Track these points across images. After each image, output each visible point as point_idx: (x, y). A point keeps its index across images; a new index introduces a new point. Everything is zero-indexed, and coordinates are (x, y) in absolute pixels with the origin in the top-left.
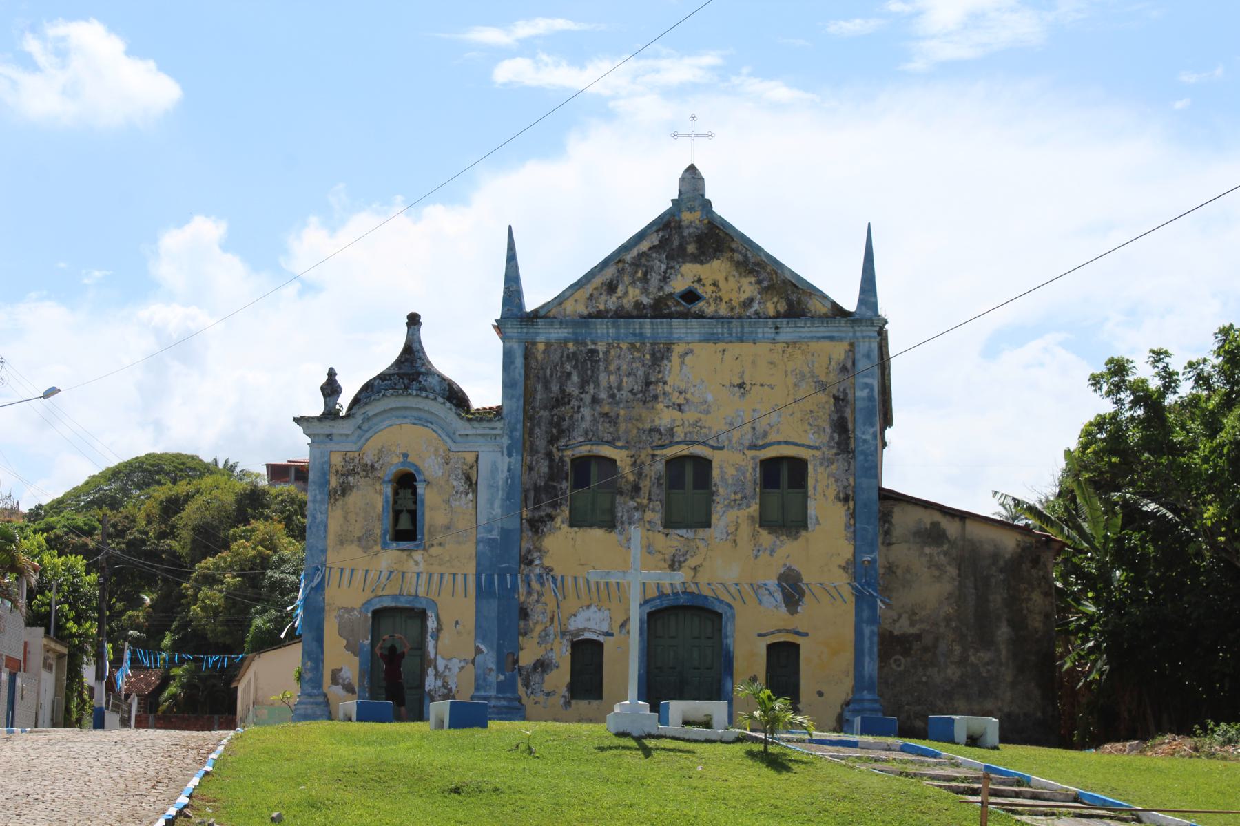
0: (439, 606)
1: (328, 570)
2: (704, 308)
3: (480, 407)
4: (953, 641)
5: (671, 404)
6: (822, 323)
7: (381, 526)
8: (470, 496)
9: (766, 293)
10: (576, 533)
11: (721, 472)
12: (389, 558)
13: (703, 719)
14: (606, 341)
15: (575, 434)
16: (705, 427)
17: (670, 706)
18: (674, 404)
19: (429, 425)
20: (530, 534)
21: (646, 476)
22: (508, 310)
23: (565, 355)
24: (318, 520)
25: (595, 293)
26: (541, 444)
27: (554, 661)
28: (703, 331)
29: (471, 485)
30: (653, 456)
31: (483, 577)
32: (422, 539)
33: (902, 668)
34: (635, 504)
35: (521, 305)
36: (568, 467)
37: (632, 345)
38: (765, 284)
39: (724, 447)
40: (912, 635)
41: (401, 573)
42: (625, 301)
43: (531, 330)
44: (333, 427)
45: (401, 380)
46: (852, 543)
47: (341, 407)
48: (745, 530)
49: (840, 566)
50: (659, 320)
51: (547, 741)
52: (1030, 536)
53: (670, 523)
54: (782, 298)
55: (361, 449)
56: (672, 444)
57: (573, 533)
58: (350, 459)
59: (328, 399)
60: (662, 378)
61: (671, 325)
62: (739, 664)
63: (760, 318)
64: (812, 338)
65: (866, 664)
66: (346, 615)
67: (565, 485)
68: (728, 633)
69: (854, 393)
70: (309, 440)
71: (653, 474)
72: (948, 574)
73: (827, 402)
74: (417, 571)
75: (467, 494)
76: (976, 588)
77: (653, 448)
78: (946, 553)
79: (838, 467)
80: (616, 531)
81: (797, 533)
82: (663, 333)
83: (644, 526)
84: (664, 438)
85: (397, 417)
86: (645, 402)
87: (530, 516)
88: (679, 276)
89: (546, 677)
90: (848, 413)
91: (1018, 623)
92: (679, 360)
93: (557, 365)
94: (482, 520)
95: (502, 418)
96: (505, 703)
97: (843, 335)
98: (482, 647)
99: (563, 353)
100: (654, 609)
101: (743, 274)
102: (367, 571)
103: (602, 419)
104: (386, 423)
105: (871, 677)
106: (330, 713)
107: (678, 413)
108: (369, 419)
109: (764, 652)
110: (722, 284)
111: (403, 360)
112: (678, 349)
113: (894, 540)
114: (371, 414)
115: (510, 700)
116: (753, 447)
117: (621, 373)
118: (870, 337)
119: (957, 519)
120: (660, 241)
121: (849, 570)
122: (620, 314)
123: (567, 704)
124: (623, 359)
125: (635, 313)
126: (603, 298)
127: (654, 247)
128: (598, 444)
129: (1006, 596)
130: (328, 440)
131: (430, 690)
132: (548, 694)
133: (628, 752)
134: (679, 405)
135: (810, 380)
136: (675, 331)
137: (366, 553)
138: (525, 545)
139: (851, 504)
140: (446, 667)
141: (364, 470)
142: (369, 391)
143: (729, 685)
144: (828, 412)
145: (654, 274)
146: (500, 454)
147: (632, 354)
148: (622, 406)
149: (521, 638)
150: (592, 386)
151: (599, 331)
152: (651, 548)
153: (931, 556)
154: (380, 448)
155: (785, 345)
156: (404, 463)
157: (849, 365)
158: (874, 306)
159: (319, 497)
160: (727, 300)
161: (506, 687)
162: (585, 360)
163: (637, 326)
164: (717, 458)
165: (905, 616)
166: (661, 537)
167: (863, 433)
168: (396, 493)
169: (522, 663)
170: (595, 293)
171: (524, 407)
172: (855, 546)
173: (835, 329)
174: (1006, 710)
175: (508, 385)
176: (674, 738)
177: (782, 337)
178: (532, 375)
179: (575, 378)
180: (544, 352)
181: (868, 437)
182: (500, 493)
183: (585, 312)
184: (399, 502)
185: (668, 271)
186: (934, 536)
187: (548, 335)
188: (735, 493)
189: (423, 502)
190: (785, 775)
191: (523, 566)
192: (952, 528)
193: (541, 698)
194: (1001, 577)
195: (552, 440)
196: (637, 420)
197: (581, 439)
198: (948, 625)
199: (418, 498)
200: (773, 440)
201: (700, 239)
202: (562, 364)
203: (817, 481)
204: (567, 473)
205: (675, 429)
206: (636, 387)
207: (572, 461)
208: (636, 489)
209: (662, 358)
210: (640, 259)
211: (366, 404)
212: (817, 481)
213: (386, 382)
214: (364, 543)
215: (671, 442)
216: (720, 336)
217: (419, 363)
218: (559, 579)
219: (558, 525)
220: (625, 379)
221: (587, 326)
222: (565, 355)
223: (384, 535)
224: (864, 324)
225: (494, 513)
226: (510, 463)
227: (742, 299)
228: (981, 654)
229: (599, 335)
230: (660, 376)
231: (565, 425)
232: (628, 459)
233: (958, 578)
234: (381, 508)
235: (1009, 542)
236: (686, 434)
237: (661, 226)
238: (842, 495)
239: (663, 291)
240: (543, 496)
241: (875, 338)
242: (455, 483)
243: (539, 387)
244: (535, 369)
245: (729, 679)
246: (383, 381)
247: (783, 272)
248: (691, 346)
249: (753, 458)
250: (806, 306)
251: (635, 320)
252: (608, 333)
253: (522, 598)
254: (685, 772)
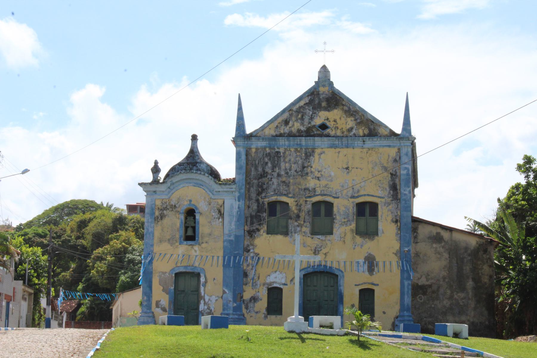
0: (206, 272)
1: (154, 254)
2: (330, 132)
3: (225, 178)
4: (446, 288)
5: (314, 177)
6: (385, 139)
7: (179, 234)
8: (221, 220)
9: (359, 125)
10: (270, 237)
11: (338, 209)
12: (183, 248)
13: (329, 325)
14: (284, 147)
15: (269, 191)
16: (330, 188)
17: (314, 318)
18: (316, 177)
19: (201, 187)
20: (248, 237)
21: (303, 211)
22: (238, 133)
23: (265, 154)
24: (150, 231)
25: (279, 125)
26: (254, 195)
27: (259, 297)
28: (329, 143)
29: (221, 214)
30: (306, 201)
31: (227, 257)
32: (198, 240)
33: (423, 301)
34: (298, 224)
35: (244, 131)
36: (266, 206)
37: (296, 150)
38: (359, 121)
39: (339, 197)
40: (427, 285)
41: (188, 256)
42: (293, 129)
43: (249, 143)
44: (157, 187)
45: (188, 166)
46: (399, 242)
47: (160, 178)
48: (349, 236)
49: (393, 253)
50: (309, 138)
51: (256, 335)
52: (483, 239)
53: (314, 233)
54: (366, 127)
55: (170, 197)
56: (315, 195)
57: (269, 237)
58: (165, 203)
59: (154, 174)
60: (310, 165)
61: (314, 140)
62: (346, 299)
63: (356, 137)
64: (380, 146)
65: (406, 299)
66: (163, 275)
67: (265, 215)
68: (341, 284)
69: (400, 172)
70: (145, 194)
71: (306, 209)
72: (444, 256)
73: (387, 176)
74: (196, 255)
75: (219, 219)
76: (457, 263)
77: (306, 198)
78: (443, 247)
79: (393, 206)
80: (289, 236)
81: (374, 237)
82: (311, 144)
83: (302, 234)
84: (311, 193)
85: (187, 183)
86: (302, 176)
87: (248, 229)
88: (318, 117)
89: (256, 304)
90: (397, 181)
91: (477, 280)
92: (318, 156)
93: (261, 158)
94: (226, 231)
95: (235, 183)
96: (236, 317)
97: (395, 144)
98: (226, 291)
99: (264, 153)
100: (306, 273)
101: (348, 116)
102: (172, 255)
103: (282, 184)
104: (181, 186)
105: (408, 305)
106: (155, 321)
107: (318, 181)
108: (173, 184)
109: (357, 293)
110: (338, 121)
111: (189, 156)
112: (318, 151)
113: (419, 241)
114: (174, 181)
115: (239, 315)
116: (353, 197)
117: (291, 162)
118: (407, 146)
119: (448, 231)
120: (309, 101)
121: (398, 255)
122: (290, 135)
123: (266, 317)
124: (292, 156)
125: (297, 134)
126: (283, 127)
127: (307, 103)
128: (280, 196)
129: (471, 267)
130: (154, 193)
131: (202, 311)
132: (257, 313)
133: (294, 340)
134: (318, 178)
135: (380, 166)
136: (316, 143)
137: (172, 246)
138: (246, 243)
139: (399, 224)
140: (209, 300)
141: (171, 208)
142: (174, 171)
143: (341, 309)
144: (388, 181)
145: (306, 116)
146: (234, 200)
147: (296, 153)
148: (291, 178)
149: (244, 286)
150: (277, 169)
151: (281, 143)
152: (305, 244)
153: (436, 248)
154: (178, 197)
155: (368, 149)
156: (189, 205)
157: (398, 159)
158: (409, 132)
159: (150, 220)
160: (341, 128)
161: (237, 309)
162: (274, 156)
163: (299, 141)
164: (336, 202)
165: (424, 276)
166: (309, 239)
167: (404, 190)
168: (186, 218)
169: (245, 298)
170: (279, 125)
171: (246, 178)
172: (400, 243)
173: (391, 142)
174: (471, 320)
175: (238, 168)
176: (315, 333)
177: (366, 146)
178: (249, 163)
179: (270, 165)
180: (255, 153)
181: (407, 192)
182: (235, 218)
183: (274, 134)
184: (188, 222)
185: (313, 115)
186: (438, 239)
187: (257, 145)
188: (344, 219)
189: (198, 224)
190: (367, 351)
191: (245, 253)
192: (446, 235)
193: (253, 314)
194: (469, 258)
195: (259, 194)
196: (298, 184)
197: (272, 193)
198: (444, 281)
199: (196, 220)
200: (362, 194)
201: (328, 100)
202: (264, 158)
203: (383, 213)
204: (266, 210)
205: (316, 189)
206: (298, 169)
207: (268, 203)
208: (298, 216)
209: (310, 155)
210: (300, 109)
211: (172, 177)
212: (383, 213)
213: (181, 167)
215: (314, 195)
216: (337, 145)
217: (197, 158)
218: (262, 258)
219: (261, 234)
220: (293, 165)
221: (275, 140)
222: (265, 154)
223: (180, 238)
224: (405, 140)
225: (232, 228)
226: (239, 205)
227: (348, 128)
228: (459, 294)
229: (281, 145)
230: (309, 164)
231: (265, 187)
232: (294, 202)
233: (449, 259)
234: (179, 225)
235: (473, 242)
236: (321, 191)
237: (310, 94)
238: (394, 220)
239: (311, 124)
240: (255, 220)
241: (410, 146)
242: (213, 214)
243: (253, 169)
244: (251, 161)
245: (341, 305)
246: (180, 166)
247: (367, 116)
248: (324, 150)
249: (353, 202)
250: (378, 131)
251: (298, 138)
252: (285, 144)
253: (245, 268)
254: (321, 349)
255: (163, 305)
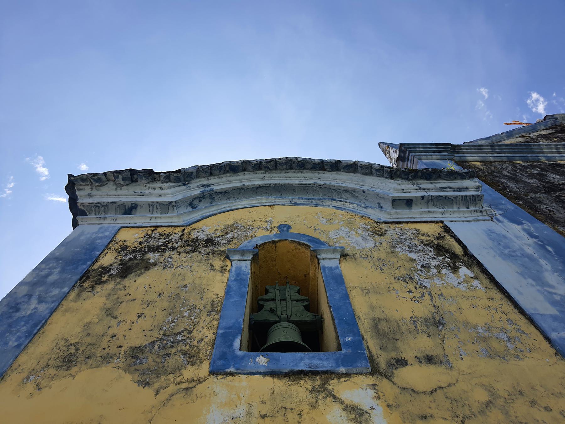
114: (216, 188)
137: (147, 384)
184: (269, 306)
214: (150, 361)
234: (222, 293)
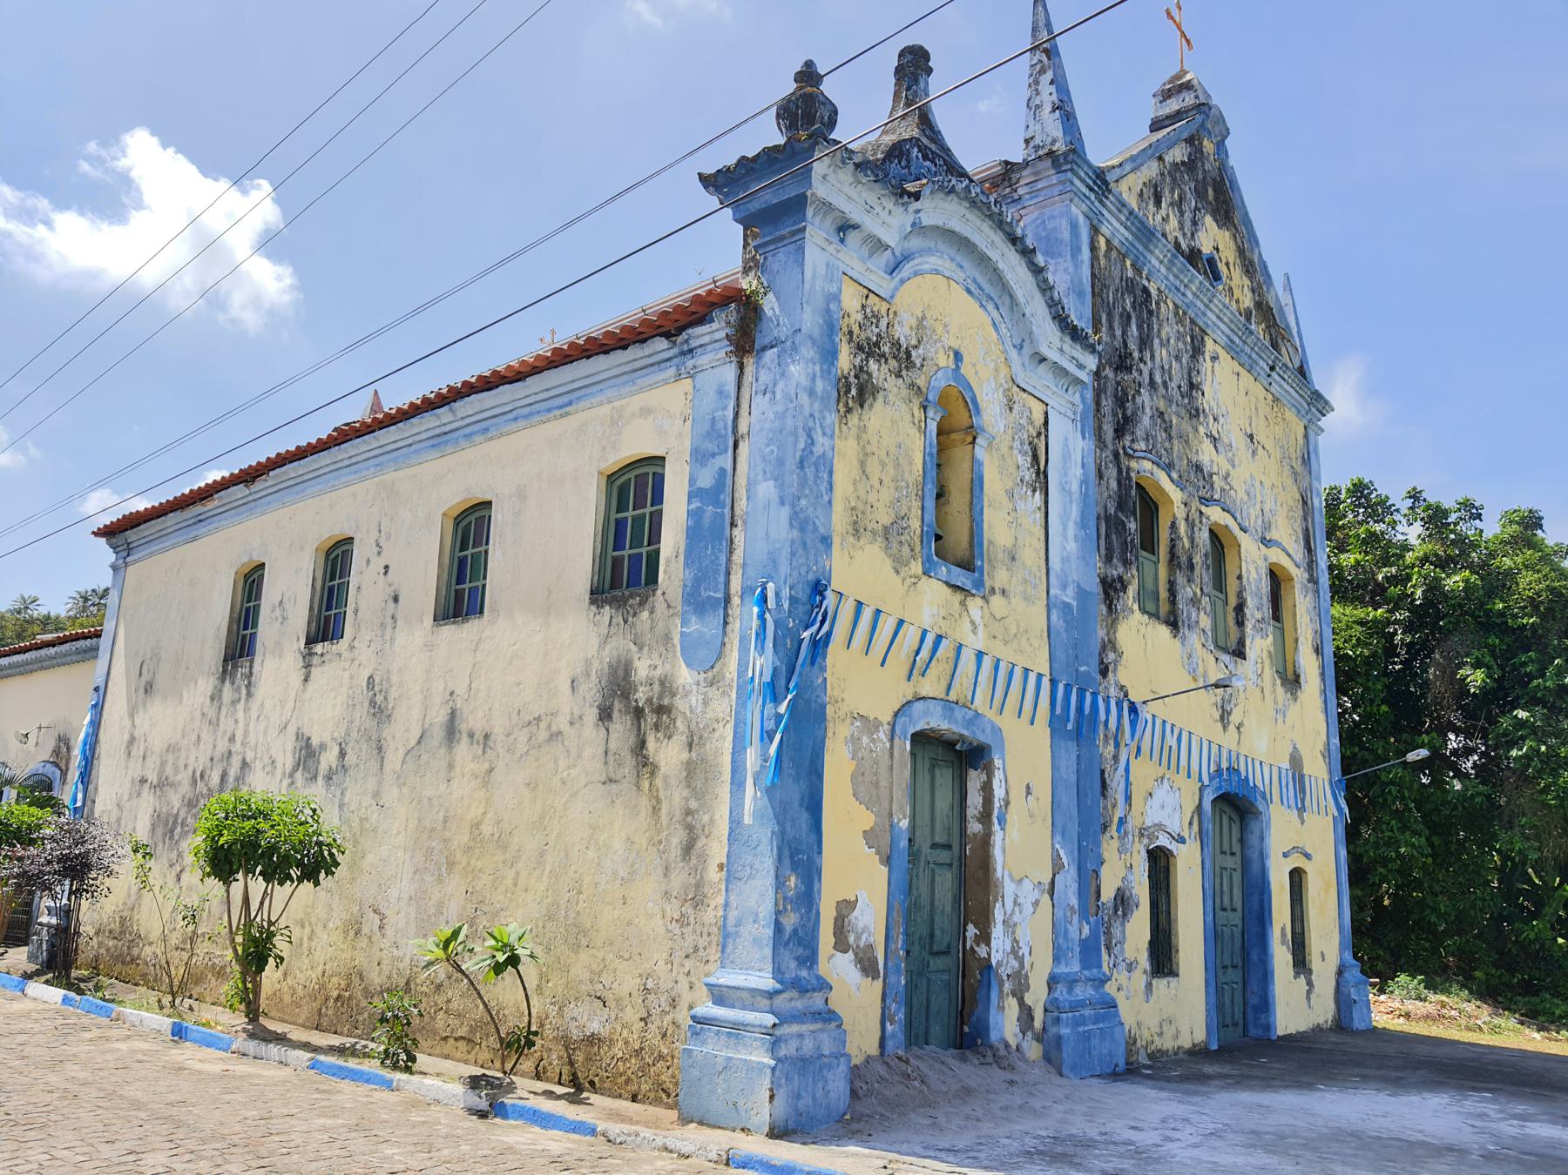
19: (990, 307)
24: (818, 450)
29: (1038, 473)
255: (865, 928)
